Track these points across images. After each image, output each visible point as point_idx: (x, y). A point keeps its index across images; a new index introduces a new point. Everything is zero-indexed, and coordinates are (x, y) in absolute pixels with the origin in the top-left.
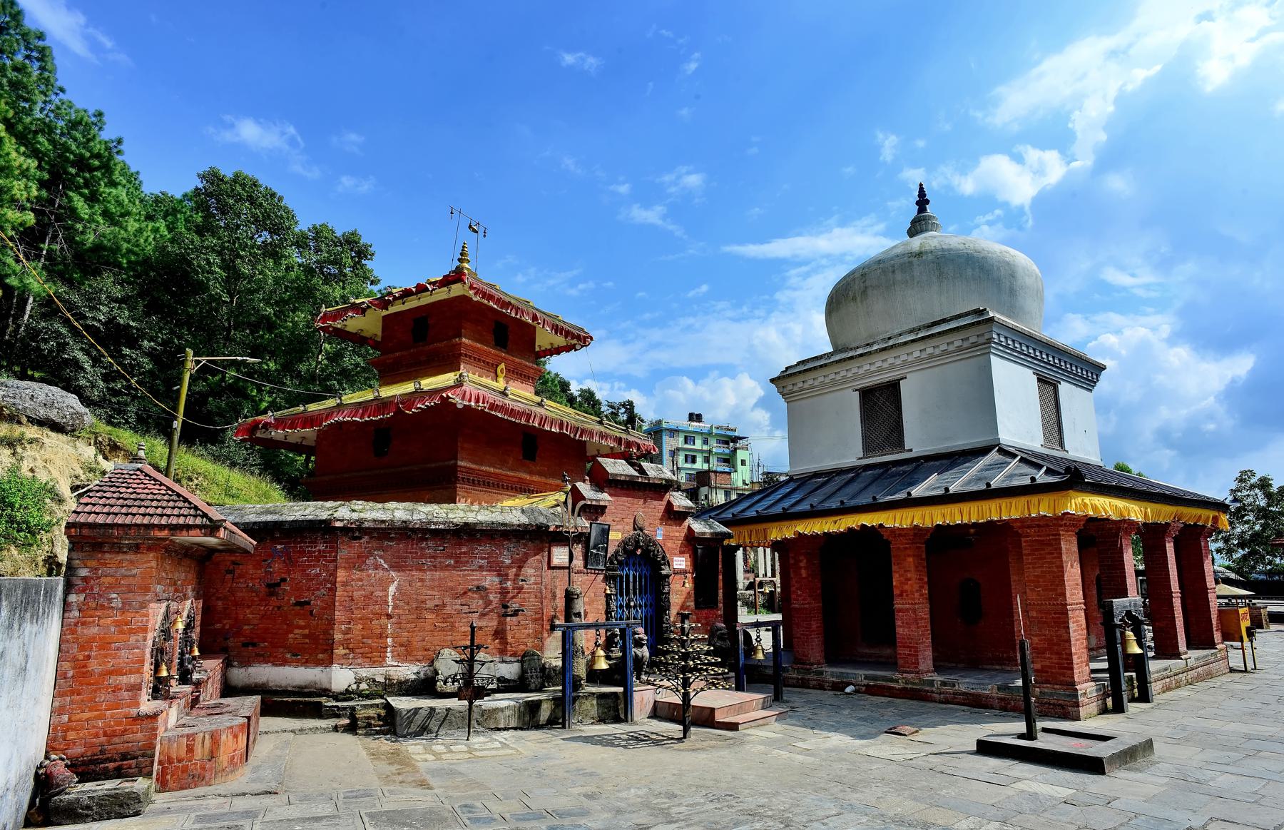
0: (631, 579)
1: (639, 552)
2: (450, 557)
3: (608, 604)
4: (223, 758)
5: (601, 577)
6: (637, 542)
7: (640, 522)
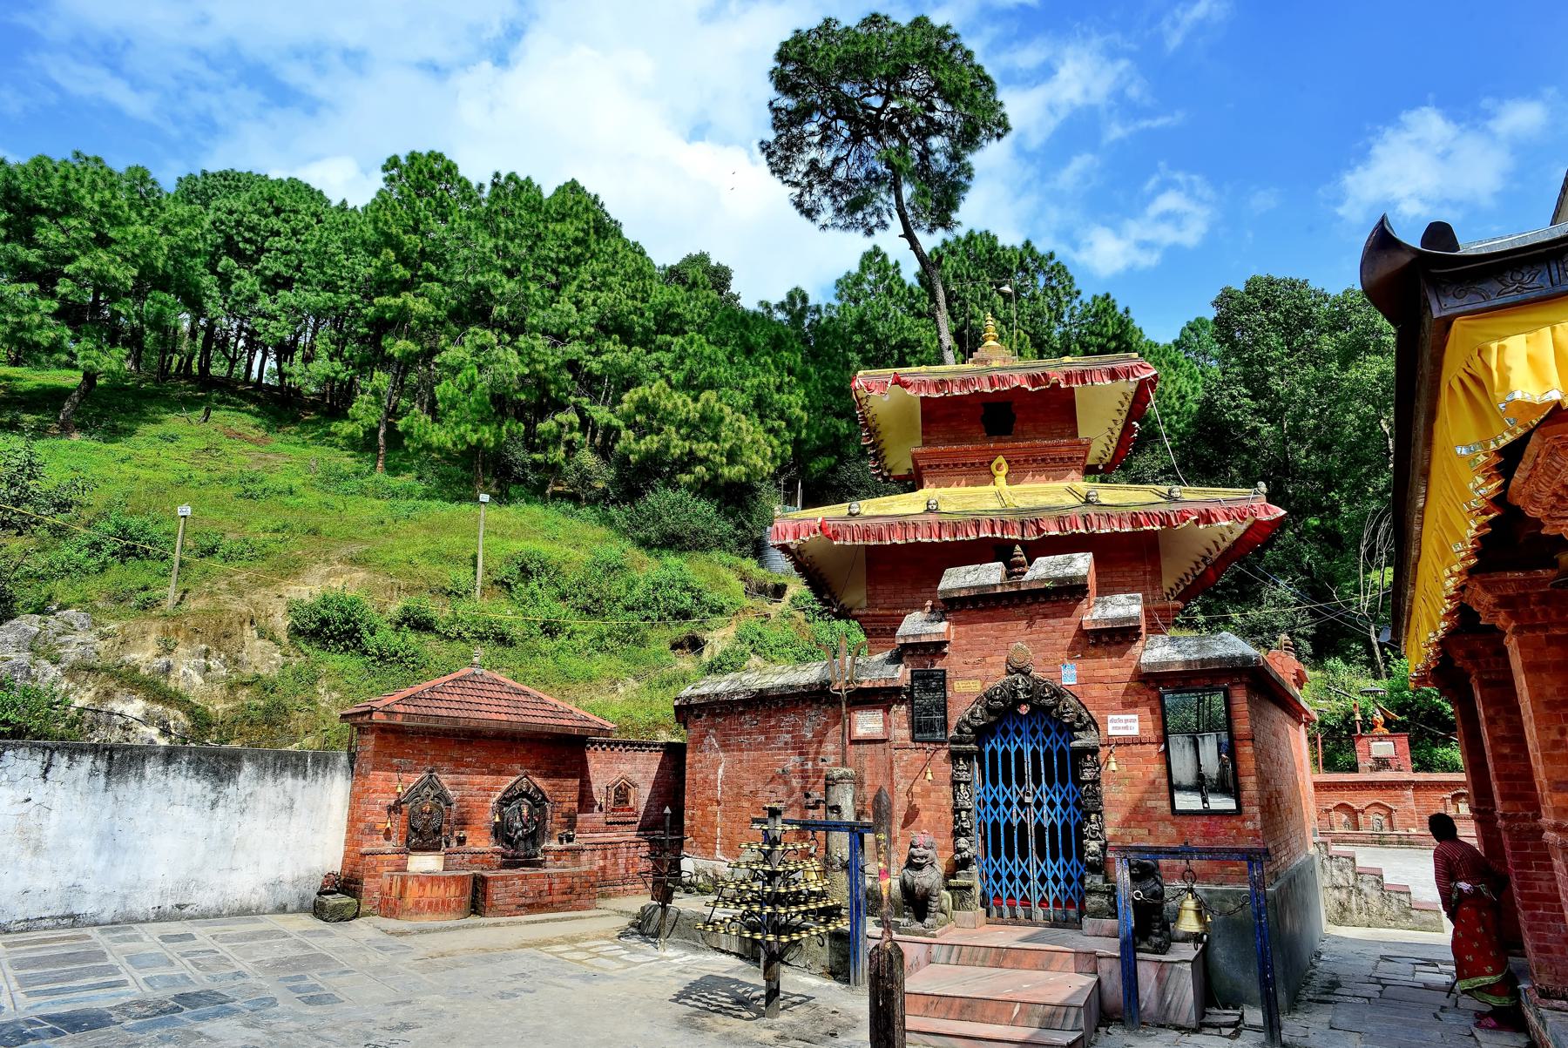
0: (1028, 758)
1: (1024, 710)
2: (761, 733)
5: (944, 753)
6: (1015, 693)
7: (1017, 660)
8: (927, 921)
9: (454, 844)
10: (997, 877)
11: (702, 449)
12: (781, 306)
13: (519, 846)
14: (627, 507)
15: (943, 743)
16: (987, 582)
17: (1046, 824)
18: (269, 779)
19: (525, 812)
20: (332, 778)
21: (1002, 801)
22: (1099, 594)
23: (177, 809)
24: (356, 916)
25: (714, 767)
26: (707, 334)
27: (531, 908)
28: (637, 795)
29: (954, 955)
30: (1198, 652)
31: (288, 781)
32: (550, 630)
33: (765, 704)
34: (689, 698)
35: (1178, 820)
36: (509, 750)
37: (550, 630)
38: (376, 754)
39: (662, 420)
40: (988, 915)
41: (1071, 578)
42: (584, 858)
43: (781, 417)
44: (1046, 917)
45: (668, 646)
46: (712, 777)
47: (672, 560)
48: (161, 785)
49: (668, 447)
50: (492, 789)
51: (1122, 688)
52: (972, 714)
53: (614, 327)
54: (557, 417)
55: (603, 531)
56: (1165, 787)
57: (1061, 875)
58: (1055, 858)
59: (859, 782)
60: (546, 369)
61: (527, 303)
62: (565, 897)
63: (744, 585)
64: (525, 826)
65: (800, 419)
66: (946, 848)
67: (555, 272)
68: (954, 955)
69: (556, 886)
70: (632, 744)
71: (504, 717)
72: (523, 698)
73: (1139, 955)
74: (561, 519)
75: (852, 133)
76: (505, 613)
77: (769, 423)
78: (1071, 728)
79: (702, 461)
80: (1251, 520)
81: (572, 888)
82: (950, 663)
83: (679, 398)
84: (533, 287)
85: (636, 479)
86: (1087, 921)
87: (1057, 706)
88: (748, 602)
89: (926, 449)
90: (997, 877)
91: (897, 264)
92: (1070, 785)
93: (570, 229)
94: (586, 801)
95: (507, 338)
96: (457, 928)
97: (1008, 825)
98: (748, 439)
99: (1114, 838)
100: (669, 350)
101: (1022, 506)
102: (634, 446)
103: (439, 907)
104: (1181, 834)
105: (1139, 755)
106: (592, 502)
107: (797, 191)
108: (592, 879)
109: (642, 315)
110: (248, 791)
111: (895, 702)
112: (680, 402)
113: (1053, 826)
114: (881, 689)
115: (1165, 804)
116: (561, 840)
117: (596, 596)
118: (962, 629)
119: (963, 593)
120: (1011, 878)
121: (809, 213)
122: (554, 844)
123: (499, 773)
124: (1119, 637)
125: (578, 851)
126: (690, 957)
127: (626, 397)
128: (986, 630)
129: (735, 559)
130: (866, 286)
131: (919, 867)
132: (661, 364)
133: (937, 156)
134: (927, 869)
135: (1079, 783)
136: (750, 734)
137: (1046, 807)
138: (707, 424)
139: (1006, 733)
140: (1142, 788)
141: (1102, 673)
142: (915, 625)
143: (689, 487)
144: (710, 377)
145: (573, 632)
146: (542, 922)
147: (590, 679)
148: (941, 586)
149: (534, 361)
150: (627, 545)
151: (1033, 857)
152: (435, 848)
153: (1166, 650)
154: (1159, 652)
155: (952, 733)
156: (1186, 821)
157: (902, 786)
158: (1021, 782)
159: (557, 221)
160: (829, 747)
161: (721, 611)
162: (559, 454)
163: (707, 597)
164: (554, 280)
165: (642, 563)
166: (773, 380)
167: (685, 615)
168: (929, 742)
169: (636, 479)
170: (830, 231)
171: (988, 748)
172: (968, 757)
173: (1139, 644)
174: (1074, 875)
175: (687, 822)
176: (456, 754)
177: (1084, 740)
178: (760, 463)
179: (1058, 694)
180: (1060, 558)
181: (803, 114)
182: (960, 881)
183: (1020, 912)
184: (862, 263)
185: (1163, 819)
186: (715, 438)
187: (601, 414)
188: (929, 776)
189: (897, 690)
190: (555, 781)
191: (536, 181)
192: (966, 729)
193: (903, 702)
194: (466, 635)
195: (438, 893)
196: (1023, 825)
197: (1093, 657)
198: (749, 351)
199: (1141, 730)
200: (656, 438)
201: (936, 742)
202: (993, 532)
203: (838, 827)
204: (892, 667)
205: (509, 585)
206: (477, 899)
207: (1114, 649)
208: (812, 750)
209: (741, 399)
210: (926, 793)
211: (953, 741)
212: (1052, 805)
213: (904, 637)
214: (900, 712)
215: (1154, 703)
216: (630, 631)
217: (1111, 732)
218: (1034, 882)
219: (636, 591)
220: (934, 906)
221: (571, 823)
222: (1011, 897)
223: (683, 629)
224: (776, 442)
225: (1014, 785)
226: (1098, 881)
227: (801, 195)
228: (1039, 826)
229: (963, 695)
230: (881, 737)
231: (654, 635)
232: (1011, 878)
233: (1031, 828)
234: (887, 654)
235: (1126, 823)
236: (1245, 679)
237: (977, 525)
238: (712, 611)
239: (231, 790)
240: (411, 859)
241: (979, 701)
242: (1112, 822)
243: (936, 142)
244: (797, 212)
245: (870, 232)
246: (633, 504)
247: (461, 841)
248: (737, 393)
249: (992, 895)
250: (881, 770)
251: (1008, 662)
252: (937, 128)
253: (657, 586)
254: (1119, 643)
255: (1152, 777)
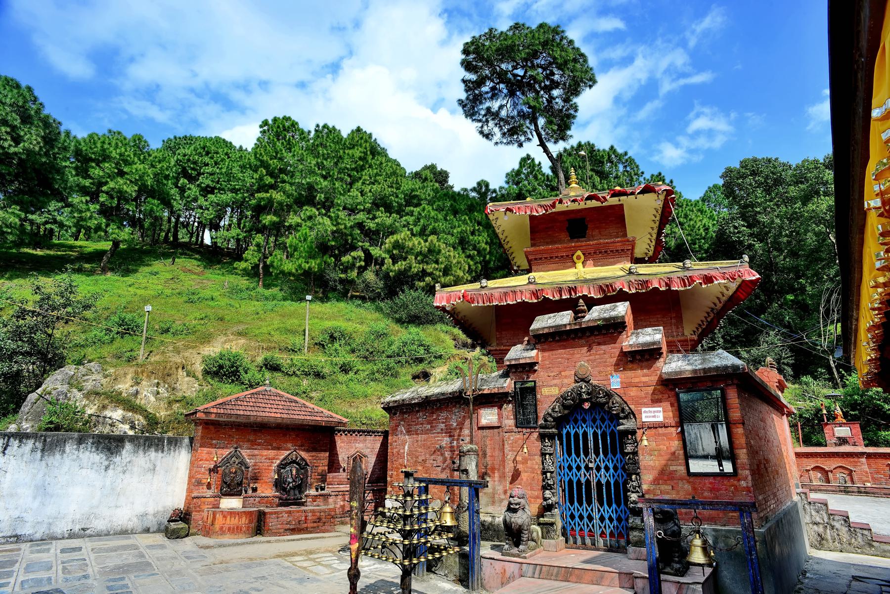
0: (591, 437)
1: (587, 406)
2: (429, 423)
3: (543, 464)
4: (217, 526)
5: (536, 435)
6: (580, 395)
8: (521, 547)
9: (250, 492)
10: (572, 517)
11: (429, 268)
12: (474, 189)
13: (290, 493)
14: (389, 302)
15: (535, 428)
16: (561, 323)
17: (603, 481)
18: (141, 452)
19: (294, 472)
20: (180, 452)
21: (574, 466)
22: (636, 327)
23: (84, 471)
24: (187, 535)
25: (405, 445)
26: (432, 205)
27: (293, 531)
28: (367, 462)
29: (537, 572)
30: (702, 364)
31: (153, 454)
32: (345, 369)
33: (430, 405)
34: (389, 403)
35: (692, 479)
36: (285, 435)
37: (345, 369)
38: (202, 438)
39: (407, 252)
40: (567, 542)
41: (614, 318)
42: (331, 500)
43: (475, 248)
44: (605, 545)
45: (410, 377)
46: (402, 451)
47: (413, 329)
48: (75, 457)
49: (410, 268)
50: (274, 459)
51: (650, 390)
52: (553, 409)
53: (382, 203)
54: (352, 254)
55: (377, 315)
56: (682, 457)
57: (614, 516)
58: (610, 505)
59: (481, 454)
60: (345, 228)
61: (335, 193)
62: (315, 525)
63: (454, 342)
64: (294, 481)
65: (485, 249)
66: (537, 497)
67: (349, 176)
68: (537, 572)
69: (309, 518)
70: (364, 432)
71: (279, 415)
72: (294, 404)
73: (663, 577)
74: (354, 309)
75: (509, 91)
76: (319, 360)
77: (468, 252)
78: (617, 417)
79: (430, 274)
80: (739, 280)
81: (320, 519)
82: (540, 377)
83: (416, 240)
84: (338, 184)
85: (395, 285)
86: (631, 549)
87: (608, 403)
88: (455, 351)
89: (533, 249)
90: (572, 517)
91: (540, 163)
92: (618, 455)
93: (357, 153)
94: (334, 465)
95: (324, 211)
96: (243, 544)
97: (579, 481)
98: (454, 261)
99: (648, 492)
100: (412, 215)
101: (588, 277)
102: (392, 267)
103: (235, 530)
104: (694, 489)
105: (664, 435)
106: (373, 300)
107: (480, 124)
108: (333, 513)
109: (397, 197)
110: (128, 460)
111: (505, 402)
112: (416, 243)
113: (608, 483)
114: (495, 393)
115: (682, 468)
116: (317, 490)
117: (371, 350)
118: (546, 354)
119: (546, 331)
120: (581, 517)
121: (488, 136)
122: (313, 492)
123: (279, 449)
124: (647, 356)
125: (326, 497)
126: (377, 566)
127: (387, 241)
128: (561, 354)
129: (449, 328)
130: (523, 176)
131: (515, 511)
132: (408, 223)
133: (557, 100)
134: (520, 512)
135: (625, 454)
136: (422, 424)
137: (603, 470)
138: (431, 254)
139: (576, 421)
140: (667, 457)
141: (637, 380)
142: (517, 353)
143: (423, 289)
144: (434, 228)
145: (358, 370)
146: (298, 540)
147: (366, 396)
148: (534, 326)
149: (338, 224)
150: (389, 322)
151: (595, 504)
152: (238, 494)
153: (680, 363)
154: (675, 365)
155: (541, 422)
156: (698, 480)
157: (510, 456)
158: (586, 454)
159: (350, 149)
160: (466, 432)
161: (440, 357)
162: (354, 274)
163: (433, 349)
164: (349, 180)
165: (398, 332)
166: (469, 229)
167: (421, 360)
168: (526, 428)
169: (395, 285)
170: (499, 145)
171: (565, 432)
172: (551, 437)
173: (661, 360)
174: (623, 516)
175: (389, 479)
176: (252, 438)
177: (627, 425)
178: (461, 274)
179: (609, 395)
180: (608, 306)
181: (480, 83)
182: (546, 519)
183: (588, 541)
184: (520, 163)
185: (682, 479)
186: (437, 262)
187: (375, 251)
188: (525, 450)
189: (506, 394)
190: (314, 454)
191: (337, 128)
192: (550, 419)
193: (510, 402)
194: (298, 373)
195: (234, 522)
196: (588, 482)
197: (631, 369)
198: (455, 212)
199: (664, 418)
200: (404, 263)
201: (530, 428)
202: (571, 294)
203: (461, 484)
204: (502, 380)
205: (323, 345)
206: (259, 525)
207: (645, 364)
208: (456, 434)
209: (451, 240)
210: (525, 461)
211: (542, 427)
212: (607, 468)
213: (510, 360)
214: (509, 408)
215: (673, 399)
216: (389, 369)
217: (644, 420)
218: (596, 521)
219: (393, 347)
220: (525, 537)
221: (323, 479)
222: (581, 530)
223: (420, 368)
224: (472, 263)
225: (582, 456)
226: (638, 521)
227: (482, 127)
228: (599, 483)
229: (548, 397)
230: (496, 425)
231: (402, 371)
232: (581, 517)
233: (594, 484)
234: (501, 372)
235: (656, 481)
236: (736, 382)
237: (560, 291)
238: (435, 357)
239: (117, 459)
240: (222, 500)
241: (557, 400)
242: (647, 478)
243: (556, 93)
244: (481, 136)
245: (521, 145)
246: (391, 299)
247: (255, 490)
248: (449, 236)
249: (569, 528)
250: (497, 446)
251: (575, 375)
252: (555, 85)
253: (405, 344)
254: (647, 360)
255: (673, 450)
